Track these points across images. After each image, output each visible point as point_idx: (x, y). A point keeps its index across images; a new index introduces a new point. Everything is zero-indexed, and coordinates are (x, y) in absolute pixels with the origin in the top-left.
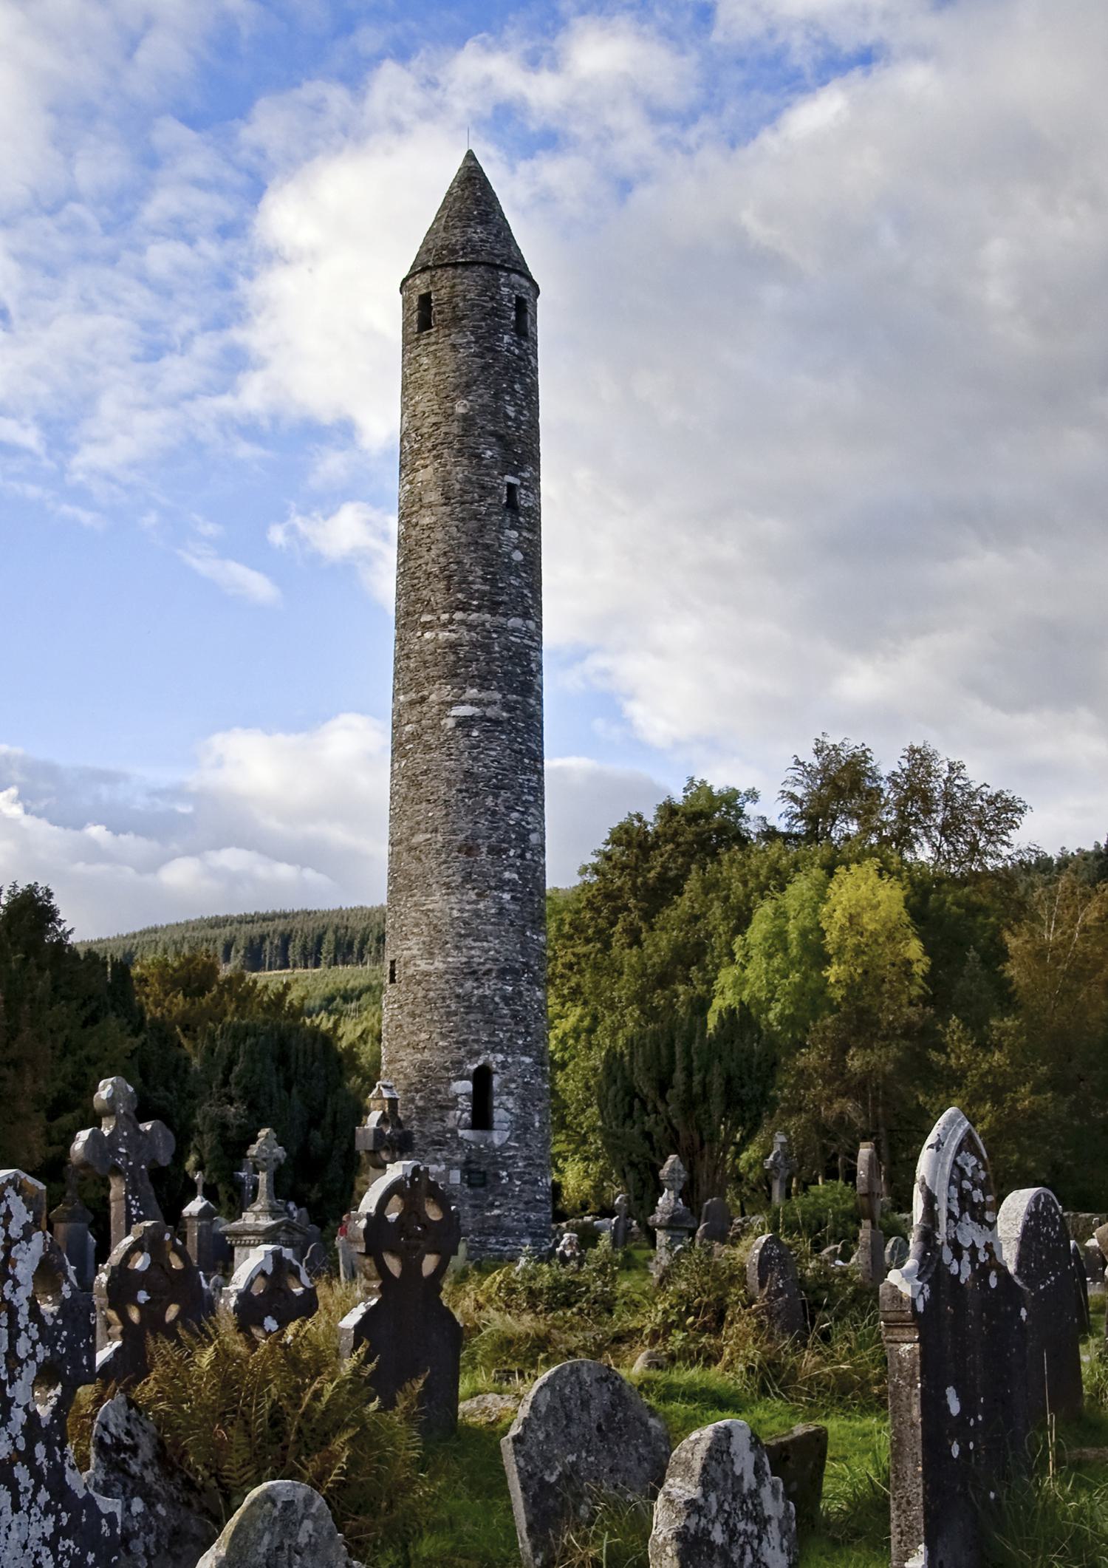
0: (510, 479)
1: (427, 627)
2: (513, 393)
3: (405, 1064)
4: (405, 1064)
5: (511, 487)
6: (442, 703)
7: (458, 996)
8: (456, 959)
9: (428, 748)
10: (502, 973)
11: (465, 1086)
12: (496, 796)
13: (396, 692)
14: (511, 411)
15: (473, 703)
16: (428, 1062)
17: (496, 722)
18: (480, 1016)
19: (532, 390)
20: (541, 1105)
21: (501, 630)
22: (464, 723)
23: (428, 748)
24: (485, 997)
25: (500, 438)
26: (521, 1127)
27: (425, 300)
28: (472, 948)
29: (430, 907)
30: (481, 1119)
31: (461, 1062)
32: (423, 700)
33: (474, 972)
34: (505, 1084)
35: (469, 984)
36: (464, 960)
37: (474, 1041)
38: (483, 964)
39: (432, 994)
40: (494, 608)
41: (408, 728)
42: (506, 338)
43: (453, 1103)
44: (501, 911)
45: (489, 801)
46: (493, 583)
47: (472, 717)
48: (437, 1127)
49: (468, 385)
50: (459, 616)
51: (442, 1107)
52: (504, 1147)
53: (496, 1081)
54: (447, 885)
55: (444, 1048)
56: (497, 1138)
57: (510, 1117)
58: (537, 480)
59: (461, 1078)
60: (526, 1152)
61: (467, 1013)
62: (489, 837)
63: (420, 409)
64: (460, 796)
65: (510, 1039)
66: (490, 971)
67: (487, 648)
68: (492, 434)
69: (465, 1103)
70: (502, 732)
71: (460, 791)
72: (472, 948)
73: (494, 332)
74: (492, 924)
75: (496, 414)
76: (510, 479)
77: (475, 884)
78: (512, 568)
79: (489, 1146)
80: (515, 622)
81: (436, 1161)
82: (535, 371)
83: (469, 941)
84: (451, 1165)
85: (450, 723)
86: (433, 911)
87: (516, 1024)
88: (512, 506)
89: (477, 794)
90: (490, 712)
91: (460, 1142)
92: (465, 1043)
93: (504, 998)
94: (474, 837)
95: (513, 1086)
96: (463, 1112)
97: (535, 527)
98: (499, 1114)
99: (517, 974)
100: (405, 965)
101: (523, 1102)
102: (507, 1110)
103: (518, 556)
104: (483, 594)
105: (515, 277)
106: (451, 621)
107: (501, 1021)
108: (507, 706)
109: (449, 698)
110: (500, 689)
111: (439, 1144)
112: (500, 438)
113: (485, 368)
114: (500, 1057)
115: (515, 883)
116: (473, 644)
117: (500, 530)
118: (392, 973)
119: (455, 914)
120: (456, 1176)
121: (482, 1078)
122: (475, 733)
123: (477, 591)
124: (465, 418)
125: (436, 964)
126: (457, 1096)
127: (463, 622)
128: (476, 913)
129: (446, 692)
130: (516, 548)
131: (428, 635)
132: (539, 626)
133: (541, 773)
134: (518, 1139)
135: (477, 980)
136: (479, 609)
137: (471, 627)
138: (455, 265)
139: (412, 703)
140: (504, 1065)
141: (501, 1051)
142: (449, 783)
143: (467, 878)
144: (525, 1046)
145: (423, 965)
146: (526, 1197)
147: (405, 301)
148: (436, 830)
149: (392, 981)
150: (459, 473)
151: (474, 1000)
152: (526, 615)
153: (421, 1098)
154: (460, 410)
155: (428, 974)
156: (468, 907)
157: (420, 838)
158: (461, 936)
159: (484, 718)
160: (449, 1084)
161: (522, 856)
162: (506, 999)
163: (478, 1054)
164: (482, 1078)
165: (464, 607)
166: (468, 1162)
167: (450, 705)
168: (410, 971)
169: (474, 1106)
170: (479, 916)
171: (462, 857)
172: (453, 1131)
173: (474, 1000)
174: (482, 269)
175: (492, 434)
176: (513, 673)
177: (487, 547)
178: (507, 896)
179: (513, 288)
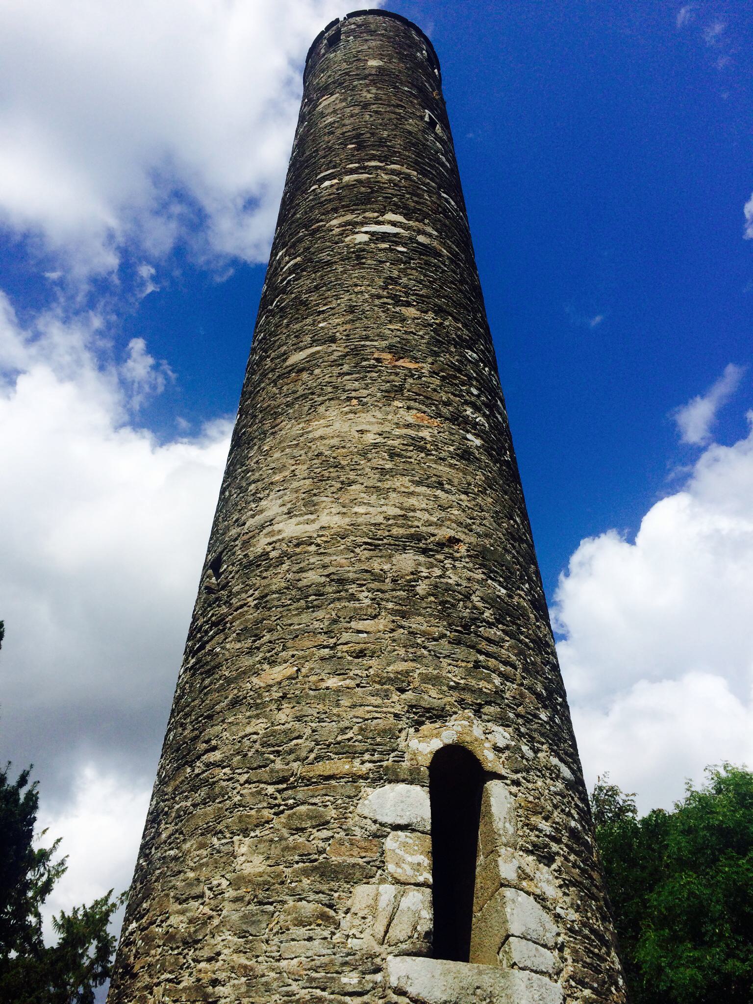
3: (216, 756)
4: (216, 756)
6: (348, 223)
7: (379, 578)
8: (373, 511)
11: (412, 802)
16: (290, 735)
24: (448, 588)
28: (412, 493)
29: (311, 436)
31: (392, 734)
33: (418, 537)
35: (407, 561)
36: (393, 511)
37: (426, 679)
38: (440, 524)
39: (312, 577)
45: (430, 316)
47: (396, 235)
50: (373, 163)
53: (499, 799)
55: (338, 691)
57: (551, 931)
61: (404, 615)
62: (436, 354)
64: (377, 302)
65: (519, 701)
66: (453, 541)
70: (445, 265)
71: (379, 297)
72: (412, 493)
74: (451, 466)
77: (412, 403)
83: (402, 482)
86: (322, 438)
87: (525, 670)
89: (408, 304)
90: (421, 239)
95: (546, 826)
98: (520, 913)
102: (540, 899)
107: (492, 649)
109: (358, 220)
114: (502, 736)
115: (483, 431)
119: (370, 438)
122: (401, 249)
123: (399, 152)
125: (325, 519)
126: (381, 831)
131: (327, 183)
135: (424, 551)
141: (504, 722)
145: (291, 529)
148: (333, 340)
151: (422, 588)
153: (255, 849)
156: (397, 432)
158: (383, 471)
159: (412, 239)
160: (354, 797)
163: (439, 715)
168: (261, 544)
169: (436, 870)
170: (422, 449)
173: (422, 588)
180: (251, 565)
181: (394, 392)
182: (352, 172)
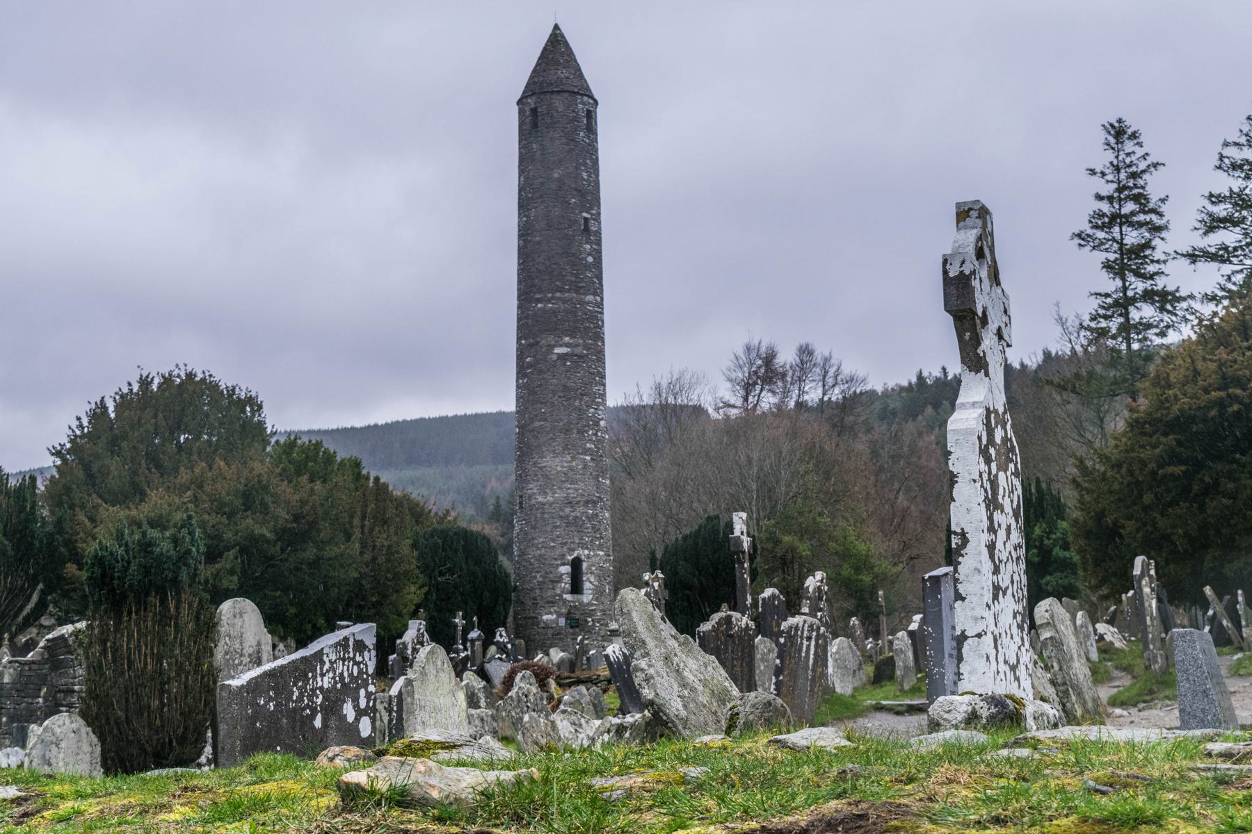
0: (585, 215)
1: (538, 301)
2: (585, 164)
5: (586, 219)
9: (541, 372)
10: (587, 502)
11: (566, 569)
12: (581, 400)
13: (519, 339)
14: (585, 175)
15: (567, 345)
17: (580, 356)
18: (573, 529)
19: (596, 162)
20: (609, 580)
21: (582, 303)
22: (562, 357)
23: (541, 372)
25: (579, 191)
26: (599, 592)
27: (534, 111)
30: (576, 588)
32: (537, 343)
34: (589, 568)
35: (568, 510)
40: (578, 290)
41: (528, 359)
42: (582, 134)
43: (560, 579)
44: (585, 467)
46: (576, 276)
47: (566, 354)
48: (550, 593)
49: (560, 161)
50: (558, 295)
51: (553, 582)
52: (590, 604)
53: (585, 565)
54: (554, 451)
56: (587, 597)
58: (599, 214)
59: (564, 564)
60: (601, 607)
63: (531, 174)
67: (574, 313)
68: (576, 189)
69: (567, 579)
73: (576, 130)
75: (578, 177)
76: (585, 215)
78: (587, 267)
79: (581, 603)
80: (590, 298)
81: (550, 613)
82: (596, 151)
84: (559, 615)
85: (555, 357)
88: (587, 229)
90: (578, 350)
91: (565, 601)
92: (566, 544)
93: (587, 517)
94: (569, 423)
96: (566, 584)
97: (599, 243)
98: (587, 585)
99: (595, 503)
100: (530, 498)
101: (599, 577)
103: (590, 259)
104: (572, 282)
105: (585, 98)
106: (553, 298)
108: (587, 347)
110: (582, 338)
111: (552, 603)
112: (579, 191)
113: (571, 151)
114: (586, 552)
116: (566, 311)
117: (580, 245)
118: (521, 503)
120: (562, 622)
121: (576, 564)
124: (559, 179)
127: (559, 299)
128: (571, 469)
129: (551, 339)
130: (589, 254)
132: (602, 299)
133: (604, 385)
134: (597, 599)
136: (569, 291)
137: (565, 301)
138: (552, 92)
139: (531, 345)
140: (588, 557)
142: (554, 393)
143: (566, 448)
144: (600, 545)
145: (540, 499)
146: (602, 633)
147: (521, 112)
148: (546, 420)
149: (521, 507)
150: (557, 212)
152: (595, 294)
154: (556, 175)
155: (544, 504)
157: (537, 424)
159: (573, 355)
161: (596, 435)
162: (589, 518)
163: (574, 550)
164: (576, 564)
165: (561, 290)
166: (569, 613)
167: (555, 346)
168: (533, 502)
171: (562, 436)
172: (561, 596)
174: (567, 95)
175: (576, 189)
176: (589, 328)
177: (574, 255)
178: (588, 458)
179: (584, 104)
180: (531, 507)
181: (566, 448)
182: (549, 301)
